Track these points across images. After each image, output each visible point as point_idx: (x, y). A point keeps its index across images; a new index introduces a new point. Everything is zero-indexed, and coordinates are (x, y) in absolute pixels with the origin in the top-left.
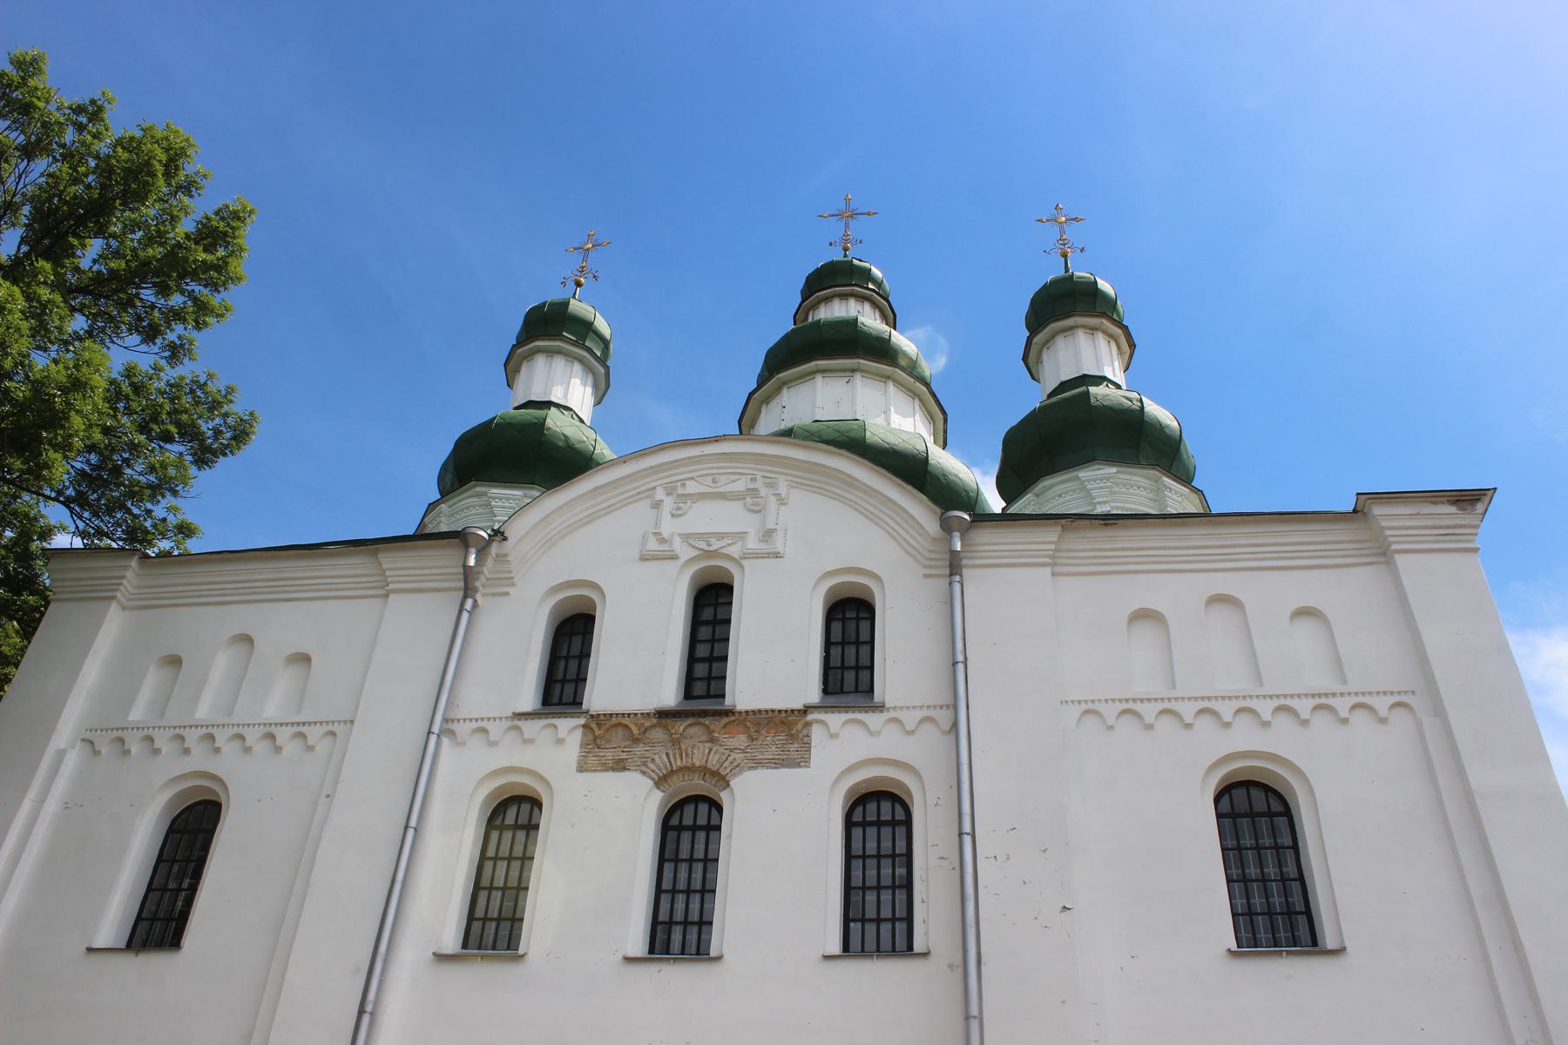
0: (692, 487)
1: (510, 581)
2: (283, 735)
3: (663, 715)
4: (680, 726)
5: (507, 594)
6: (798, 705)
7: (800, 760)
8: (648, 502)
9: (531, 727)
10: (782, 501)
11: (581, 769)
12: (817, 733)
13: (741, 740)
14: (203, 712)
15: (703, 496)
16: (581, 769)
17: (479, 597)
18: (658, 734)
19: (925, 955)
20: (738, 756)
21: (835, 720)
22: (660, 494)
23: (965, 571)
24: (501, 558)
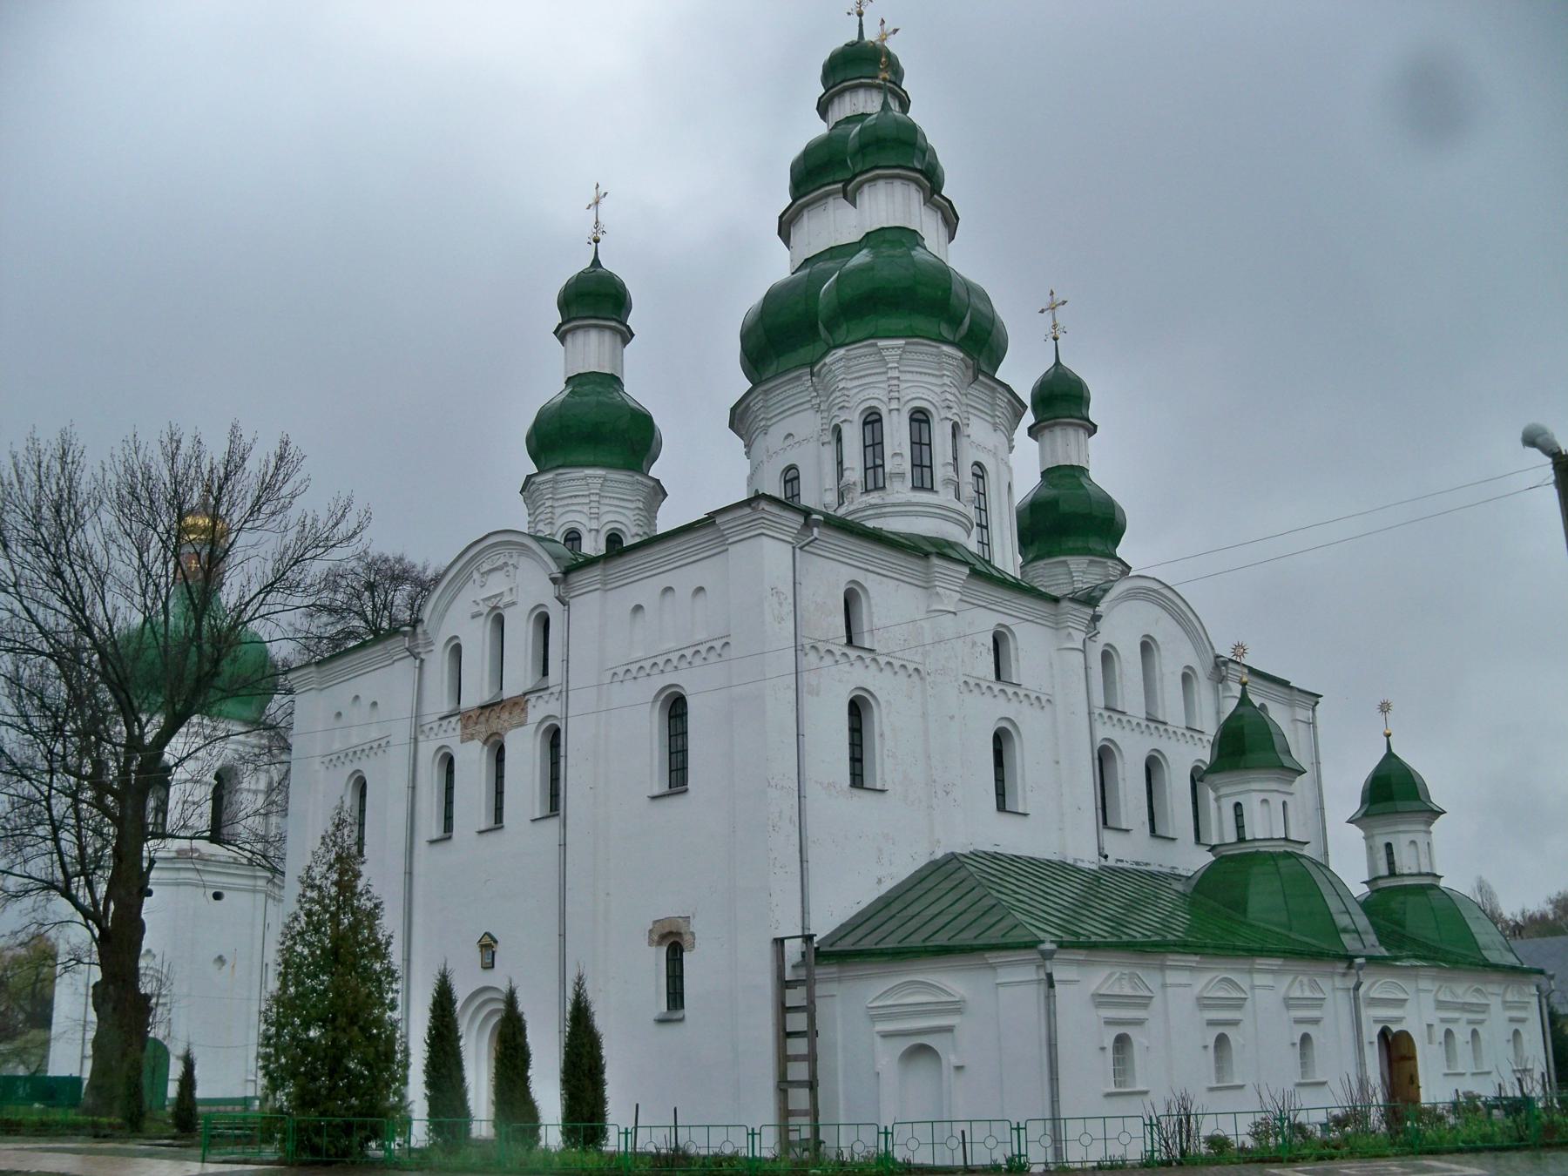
0: (486, 567)
5: (432, 651)
6: (520, 693)
7: (522, 724)
10: (516, 567)
11: (462, 742)
13: (505, 716)
15: (490, 571)
16: (462, 742)
17: (423, 656)
23: (572, 601)
24: (425, 632)
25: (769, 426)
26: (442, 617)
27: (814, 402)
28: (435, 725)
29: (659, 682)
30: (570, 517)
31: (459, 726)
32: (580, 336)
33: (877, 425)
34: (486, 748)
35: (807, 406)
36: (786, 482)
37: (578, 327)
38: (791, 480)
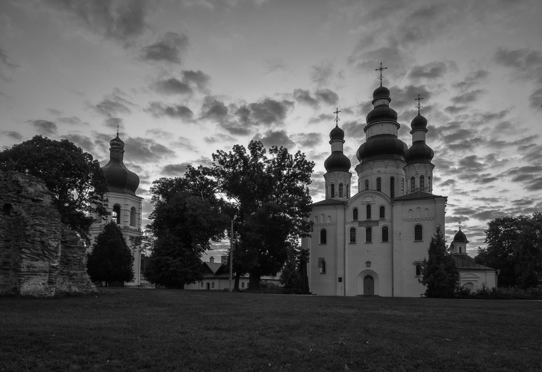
0: (366, 195)
1: (349, 207)
2: (330, 224)
3: (366, 221)
4: (367, 222)
6: (377, 220)
7: (378, 225)
8: (361, 197)
9: (353, 223)
11: (359, 226)
12: (379, 223)
13: (373, 223)
14: (321, 222)
18: (365, 223)
19: (389, 242)
20: (372, 225)
21: (381, 221)
22: (363, 197)
24: (348, 205)
25: (373, 168)
26: (352, 203)
27: (385, 166)
28: (350, 223)
29: (416, 223)
30: (341, 181)
31: (358, 224)
32: (335, 143)
33: (423, 179)
34: (366, 229)
35: (384, 166)
36: (377, 180)
37: (338, 141)
38: (379, 180)
